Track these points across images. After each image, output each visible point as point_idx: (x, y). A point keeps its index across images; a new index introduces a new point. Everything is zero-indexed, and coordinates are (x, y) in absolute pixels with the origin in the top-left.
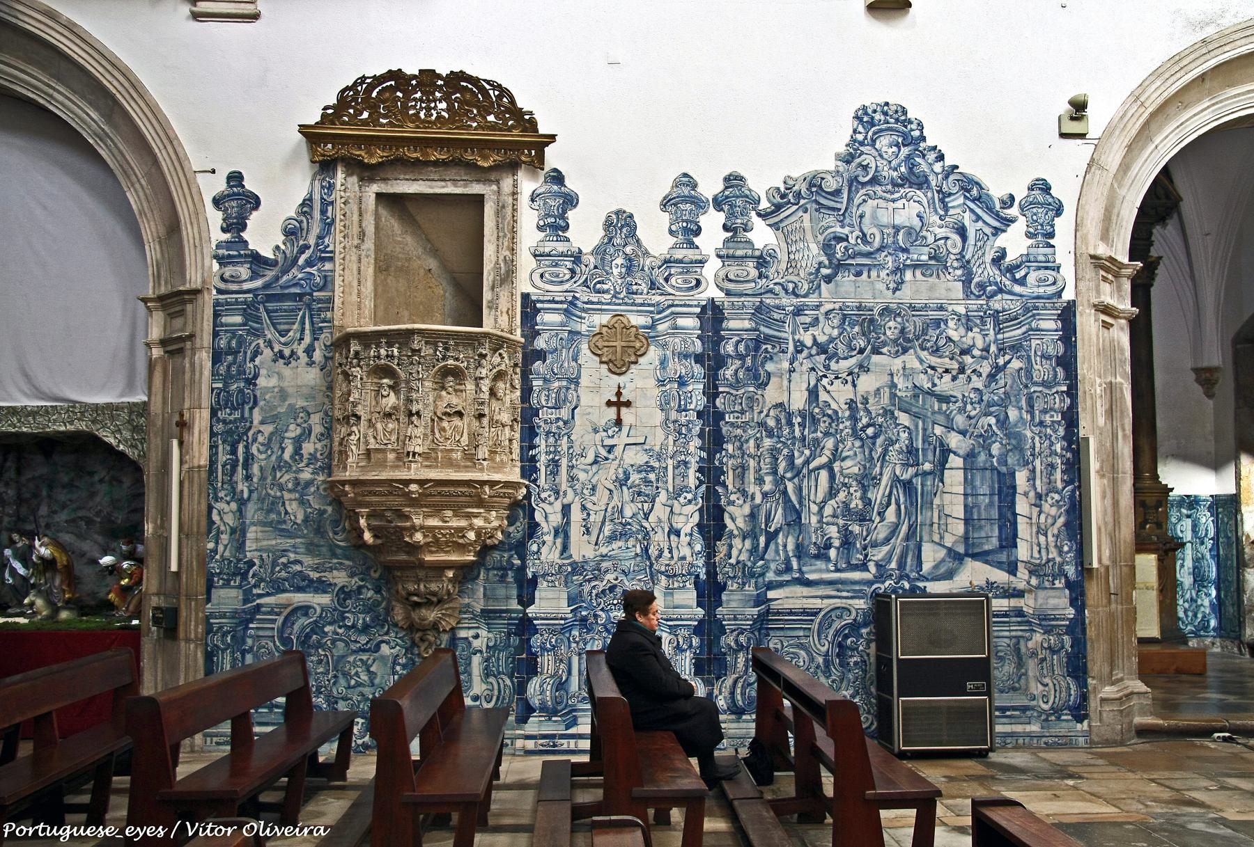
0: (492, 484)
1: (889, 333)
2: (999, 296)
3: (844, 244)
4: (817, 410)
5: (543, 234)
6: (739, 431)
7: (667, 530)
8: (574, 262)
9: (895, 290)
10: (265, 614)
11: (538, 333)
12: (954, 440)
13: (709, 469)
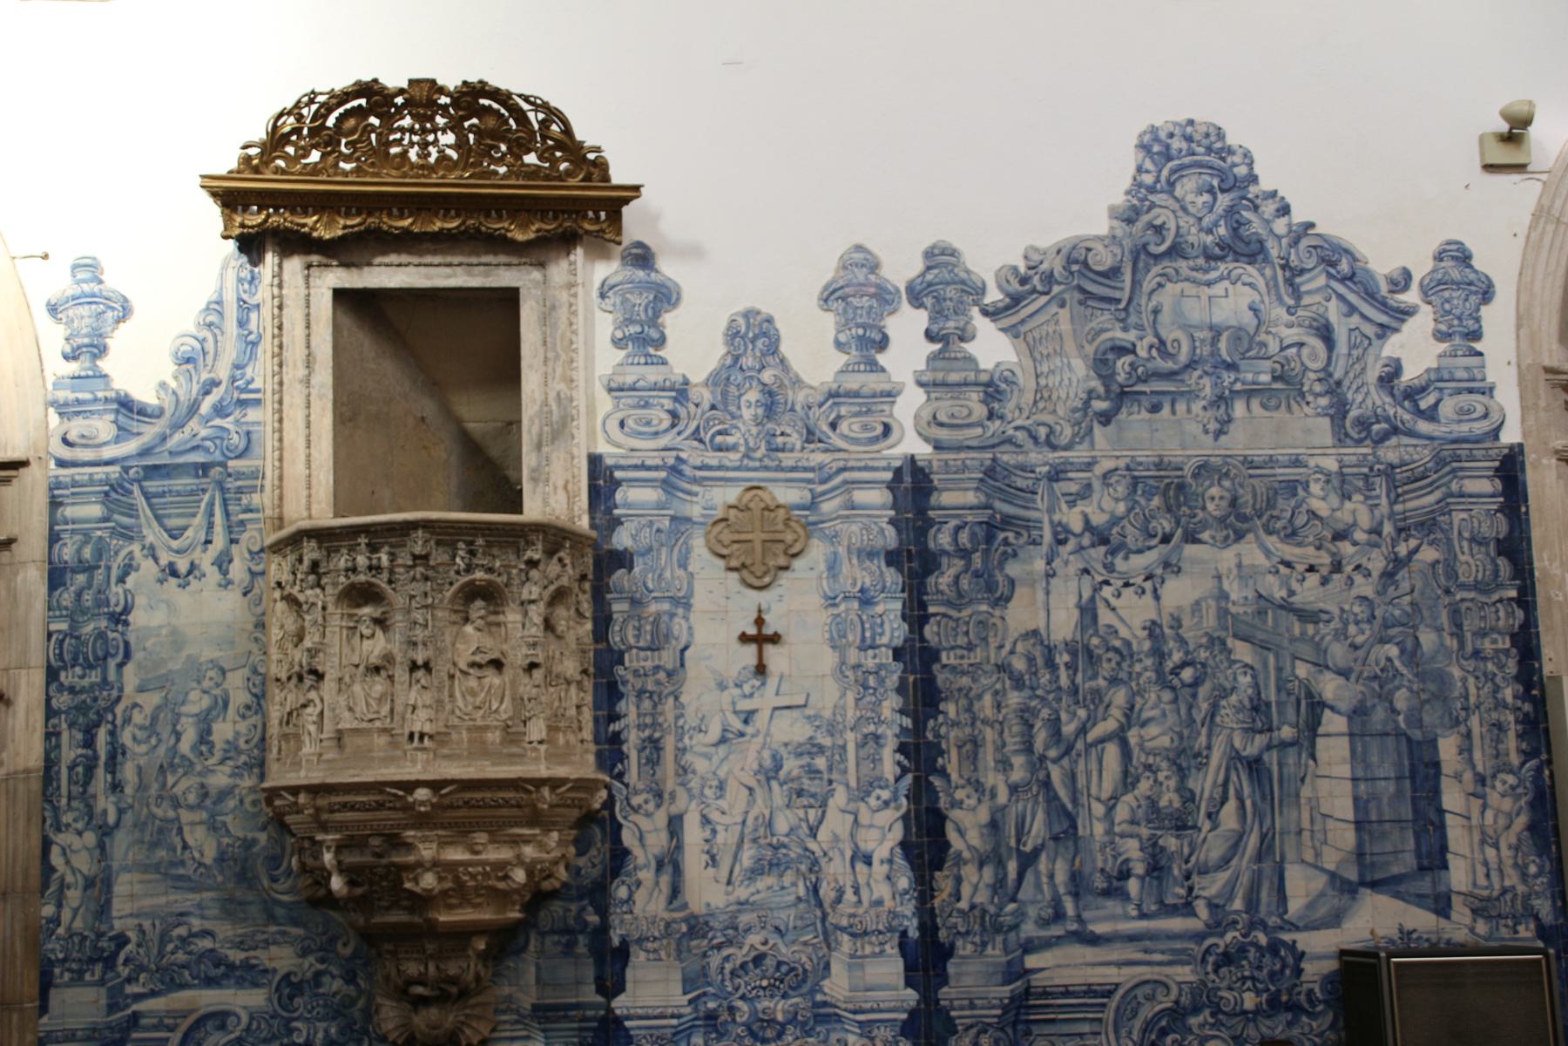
0: (554, 783)
1: (1210, 506)
2: (1394, 441)
3: (1129, 358)
4: (1095, 641)
5: (622, 353)
6: (965, 681)
7: (848, 854)
8: (675, 400)
9: (1219, 433)
10: (147, 1029)
11: (617, 522)
12: (1329, 686)
13: (917, 746)
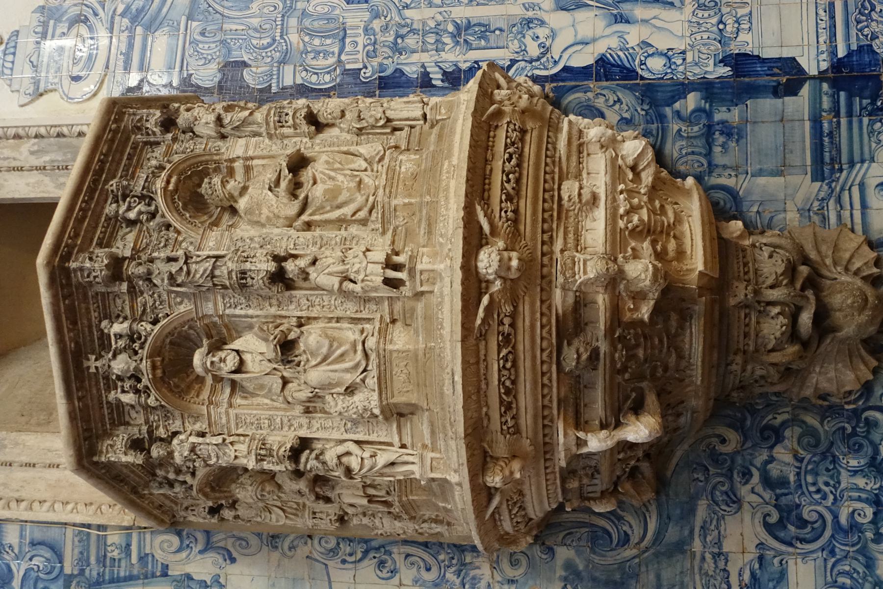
8: (58, 20)
